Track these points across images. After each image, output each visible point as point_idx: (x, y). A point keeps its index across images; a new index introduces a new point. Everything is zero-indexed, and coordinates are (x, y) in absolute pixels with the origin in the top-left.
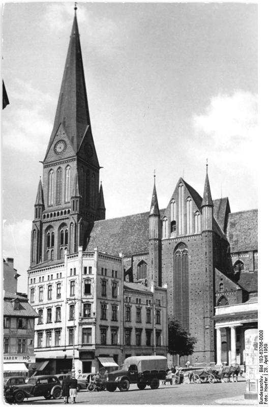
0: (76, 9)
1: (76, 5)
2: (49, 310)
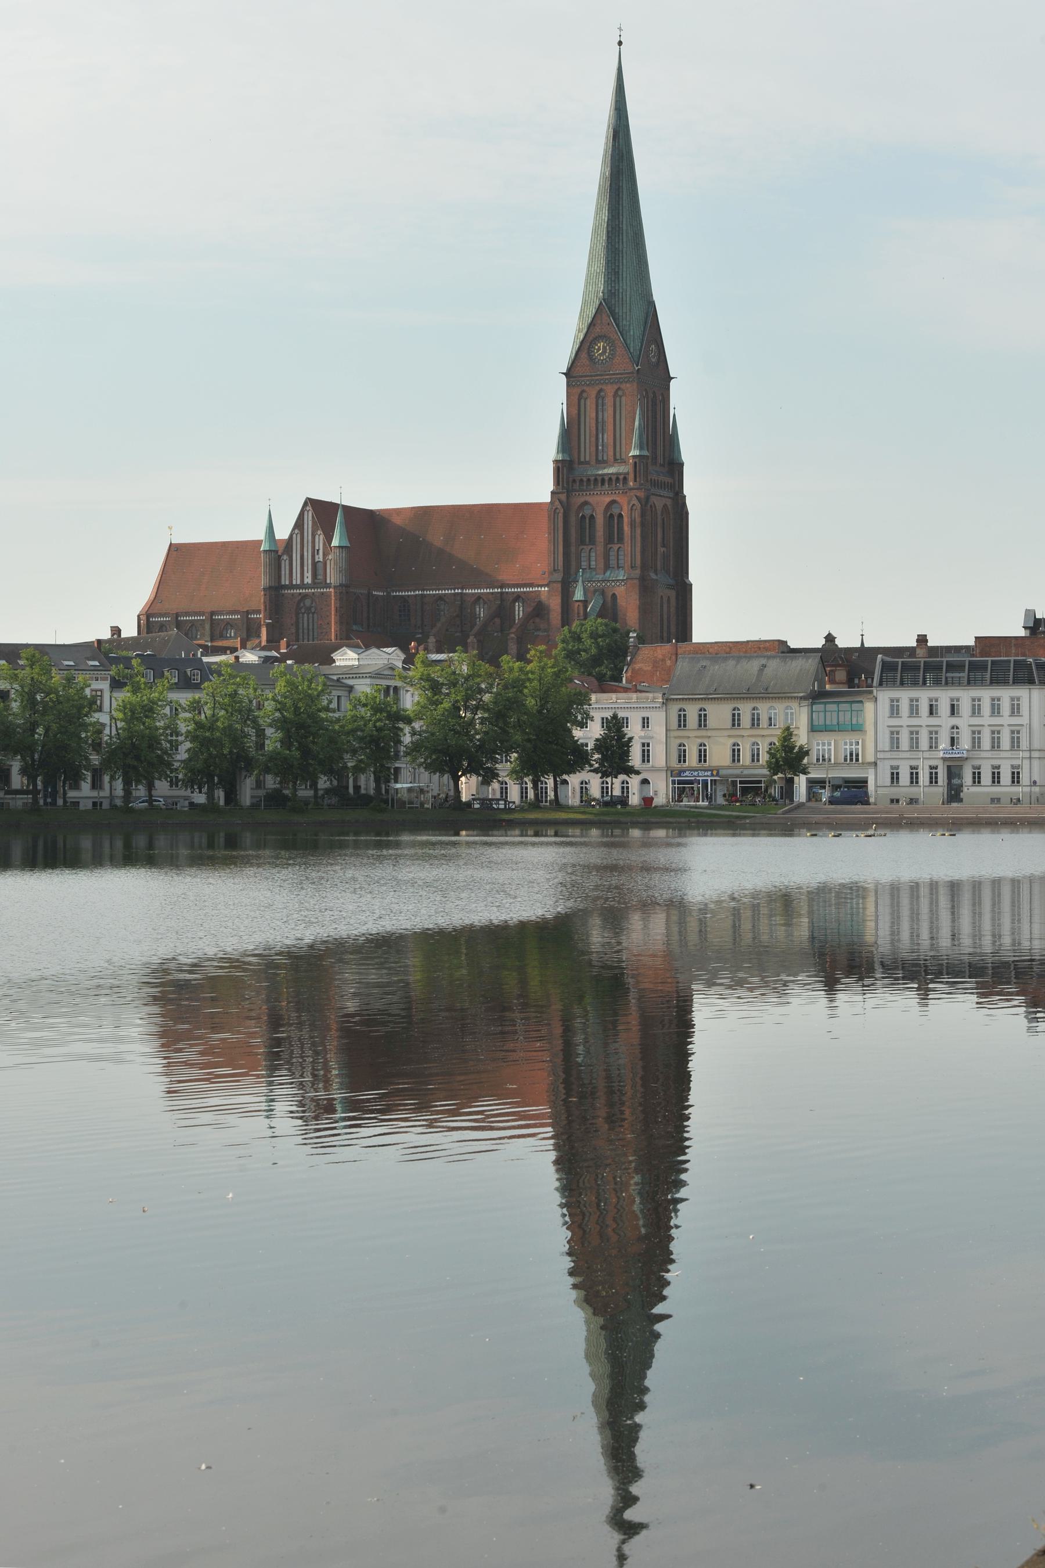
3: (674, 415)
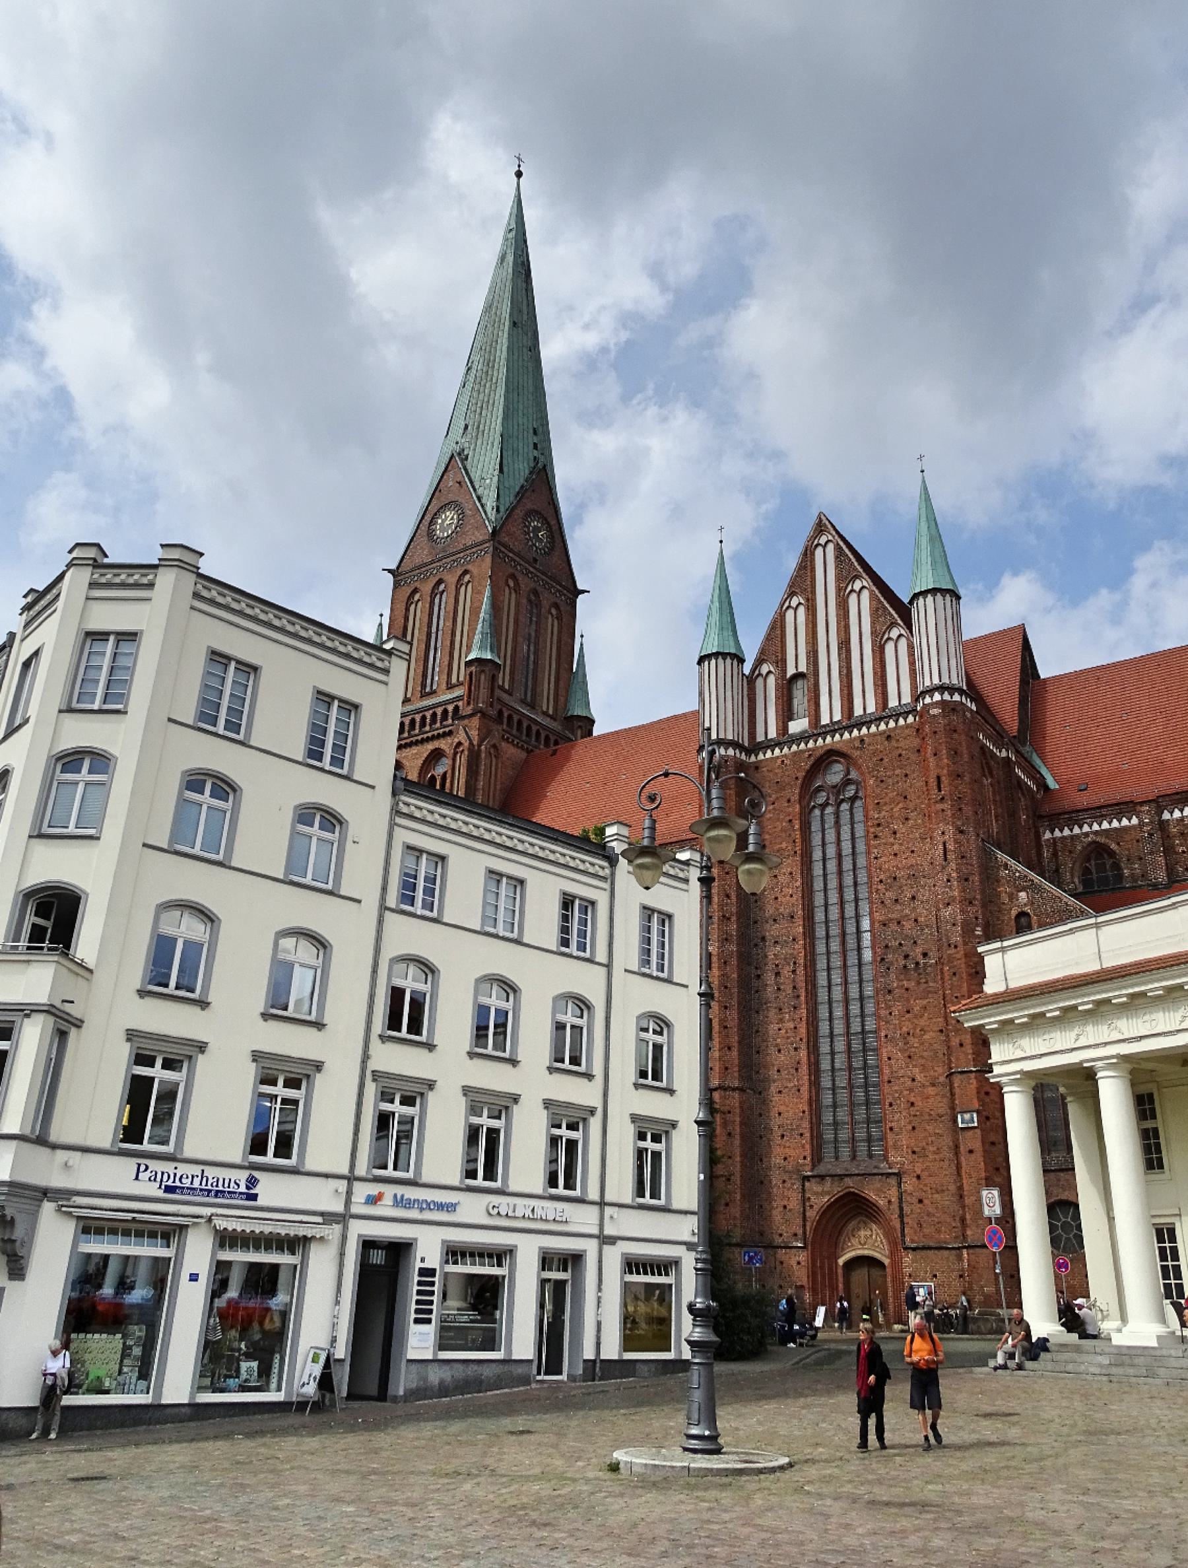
0: (519, 174)
1: (519, 166)
2: (224, 1180)
3: (582, 645)
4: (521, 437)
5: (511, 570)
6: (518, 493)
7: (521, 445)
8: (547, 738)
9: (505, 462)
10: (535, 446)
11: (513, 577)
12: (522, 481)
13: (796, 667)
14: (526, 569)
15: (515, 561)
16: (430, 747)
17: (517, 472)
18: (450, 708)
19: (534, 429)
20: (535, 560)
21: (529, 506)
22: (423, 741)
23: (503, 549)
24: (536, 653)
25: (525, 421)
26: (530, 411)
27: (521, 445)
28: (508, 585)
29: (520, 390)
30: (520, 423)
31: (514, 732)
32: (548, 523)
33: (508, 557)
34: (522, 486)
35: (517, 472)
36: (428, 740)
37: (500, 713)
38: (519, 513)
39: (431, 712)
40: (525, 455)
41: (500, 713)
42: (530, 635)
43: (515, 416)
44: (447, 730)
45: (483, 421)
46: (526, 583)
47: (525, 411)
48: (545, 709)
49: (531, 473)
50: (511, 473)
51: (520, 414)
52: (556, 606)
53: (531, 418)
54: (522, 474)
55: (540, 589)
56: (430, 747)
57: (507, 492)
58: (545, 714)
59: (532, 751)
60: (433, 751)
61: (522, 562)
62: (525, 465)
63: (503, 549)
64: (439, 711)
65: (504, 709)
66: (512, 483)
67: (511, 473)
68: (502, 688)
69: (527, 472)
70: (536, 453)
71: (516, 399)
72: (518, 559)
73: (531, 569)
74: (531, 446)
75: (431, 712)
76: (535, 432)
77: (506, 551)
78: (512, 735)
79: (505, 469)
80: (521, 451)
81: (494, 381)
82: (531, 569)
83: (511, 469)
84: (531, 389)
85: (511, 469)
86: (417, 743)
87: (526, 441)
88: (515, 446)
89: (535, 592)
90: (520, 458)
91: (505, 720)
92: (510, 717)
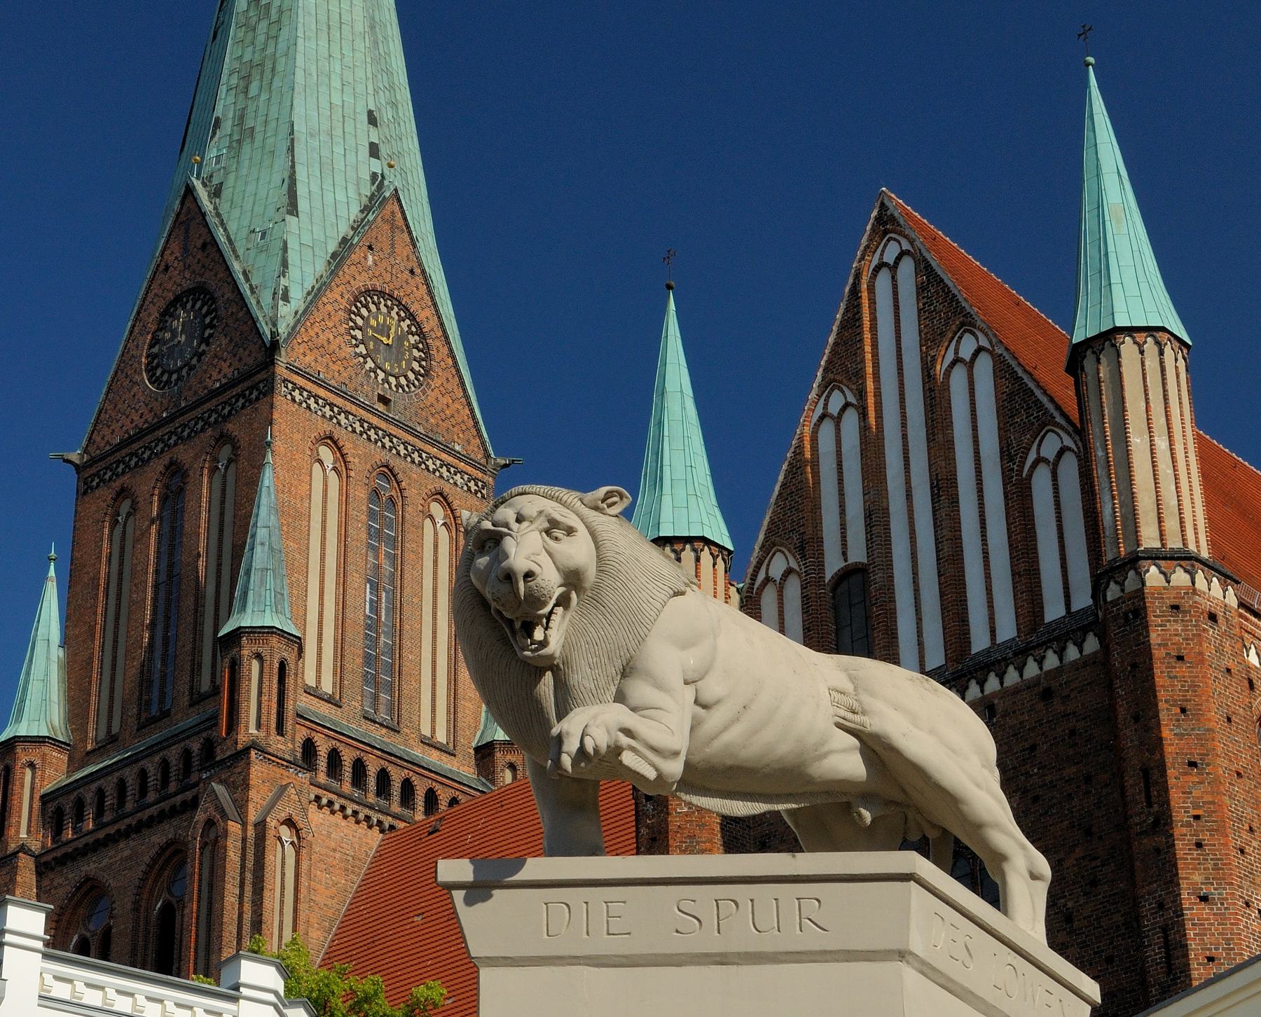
4: (338, 132)
5: (327, 427)
6: (334, 256)
7: (339, 150)
8: (431, 798)
9: (301, 190)
10: (374, 151)
11: (330, 440)
12: (344, 229)
13: (844, 554)
14: (362, 421)
15: (332, 405)
16: (158, 837)
17: (330, 211)
18: (195, 746)
19: (370, 113)
20: (383, 400)
21: (362, 282)
22: (139, 828)
23: (300, 381)
24: (392, 609)
25: (349, 99)
26: (360, 73)
27: (339, 150)
28: (320, 462)
29: (335, 34)
30: (337, 100)
31: (347, 787)
32: (412, 317)
33: (316, 397)
34: (344, 240)
35: (330, 211)
36: (150, 823)
37: (309, 748)
38: (338, 297)
39: (157, 759)
40: (351, 173)
41: (309, 748)
42: (378, 567)
43: (323, 89)
44: (189, 795)
45: (251, 109)
46: (363, 454)
47: (348, 76)
48: (426, 731)
49: (366, 209)
50: (317, 213)
51: (336, 83)
52: (441, 496)
53: (360, 88)
54: (342, 212)
55: (397, 464)
56: (158, 837)
57: (308, 253)
58: (429, 743)
59: (392, 827)
60: (163, 849)
61: (349, 407)
62: (352, 194)
63: (300, 381)
64: (173, 754)
65: (319, 739)
66: (318, 233)
67: (317, 213)
68: (313, 692)
69: (355, 212)
70: (376, 166)
71: (324, 51)
72: (338, 401)
73: (375, 421)
74: (364, 151)
75: (157, 759)
76: (372, 120)
77: (309, 386)
78: (340, 795)
79: (302, 204)
80: (339, 165)
81: (274, 17)
82: (375, 421)
83: (317, 204)
84: (359, 27)
85: (317, 204)
86: (126, 834)
87: (351, 141)
88: (326, 153)
89: (388, 472)
90: (339, 179)
91: (322, 764)
92: (334, 757)
